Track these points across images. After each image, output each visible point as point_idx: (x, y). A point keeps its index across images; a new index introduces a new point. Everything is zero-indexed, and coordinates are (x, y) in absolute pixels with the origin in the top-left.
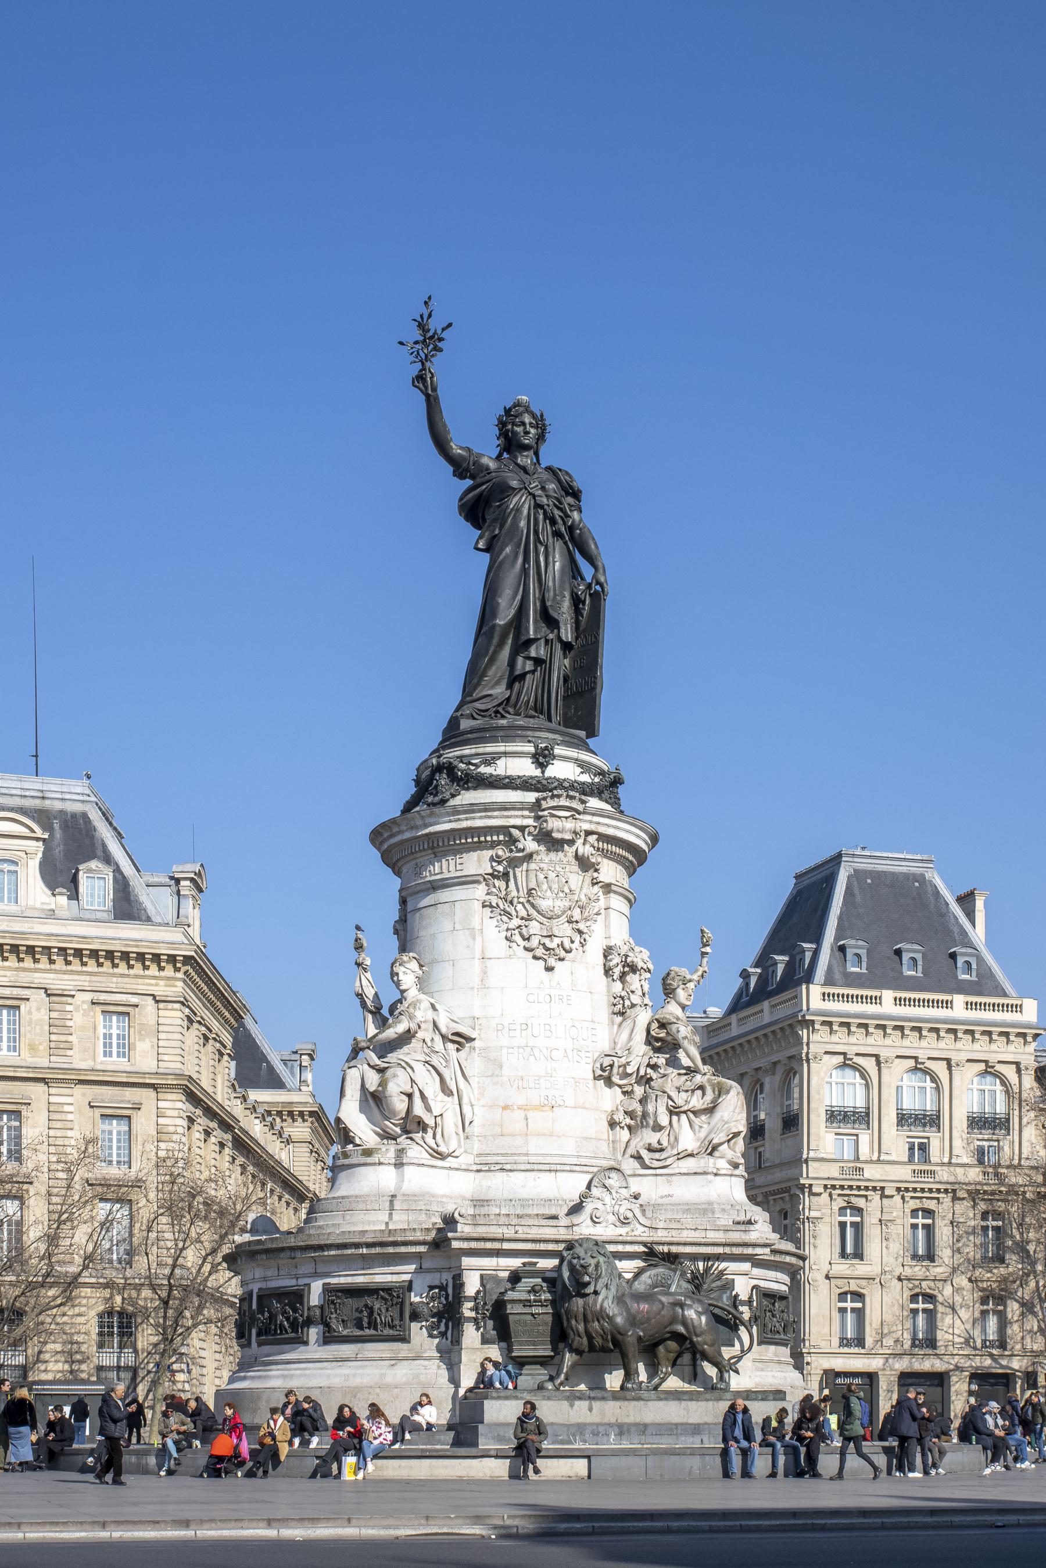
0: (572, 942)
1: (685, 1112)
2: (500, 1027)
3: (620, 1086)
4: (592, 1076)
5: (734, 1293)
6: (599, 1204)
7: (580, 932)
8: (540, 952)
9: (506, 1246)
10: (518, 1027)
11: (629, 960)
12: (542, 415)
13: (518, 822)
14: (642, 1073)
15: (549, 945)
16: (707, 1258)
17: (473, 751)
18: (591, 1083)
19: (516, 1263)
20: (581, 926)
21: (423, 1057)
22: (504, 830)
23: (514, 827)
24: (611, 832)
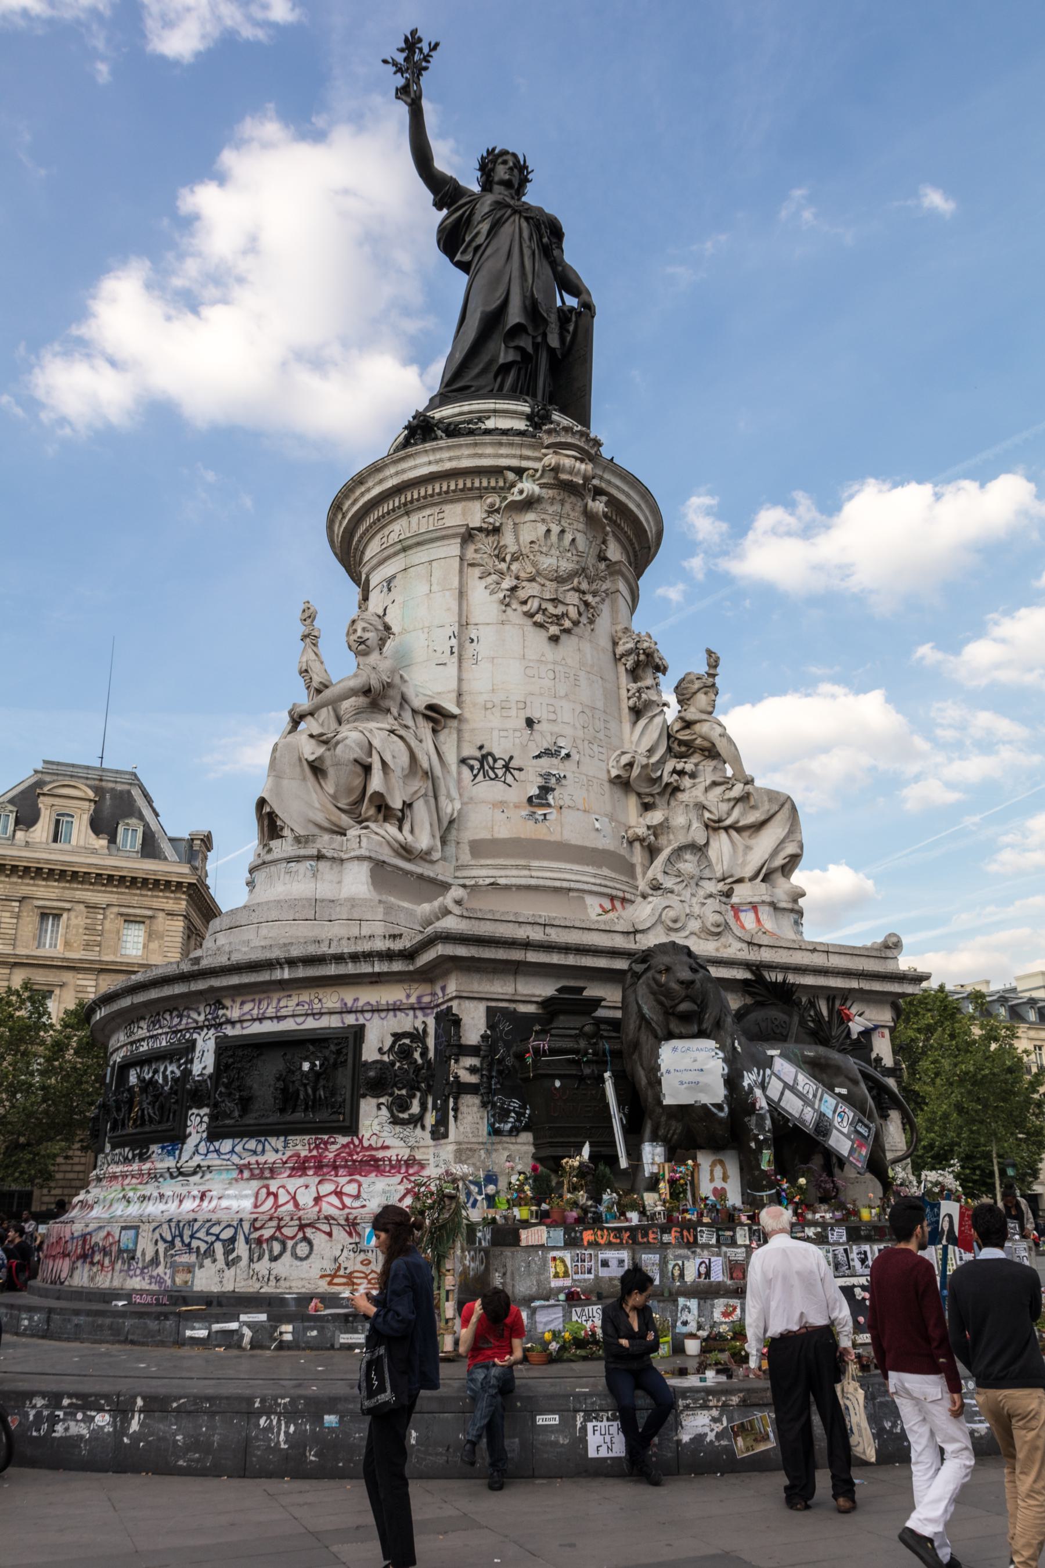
0: (580, 614)
1: (726, 829)
2: (489, 705)
3: (639, 795)
4: (605, 777)
5: (873, 1055)
6: (673, 900)
7: (587, 604)
8: (539, 618)
9: (532, 957)
10: (513, 705)
11: (645, 645)
12: (525, 161)
13: (514, 463)
14: (666, 779)
15: (551, 609)
16: (832, 995)
17: (457, 410)
18: (607, 786)
19: (546, 989)
20: (589, 598)
21: (388, 727)
22: (497, 471)
23: (509, 468)
24: (622, 498)
